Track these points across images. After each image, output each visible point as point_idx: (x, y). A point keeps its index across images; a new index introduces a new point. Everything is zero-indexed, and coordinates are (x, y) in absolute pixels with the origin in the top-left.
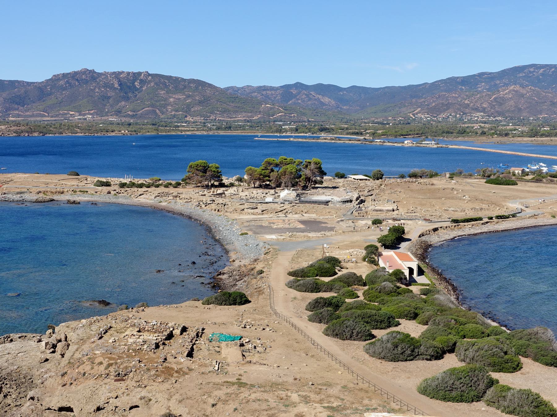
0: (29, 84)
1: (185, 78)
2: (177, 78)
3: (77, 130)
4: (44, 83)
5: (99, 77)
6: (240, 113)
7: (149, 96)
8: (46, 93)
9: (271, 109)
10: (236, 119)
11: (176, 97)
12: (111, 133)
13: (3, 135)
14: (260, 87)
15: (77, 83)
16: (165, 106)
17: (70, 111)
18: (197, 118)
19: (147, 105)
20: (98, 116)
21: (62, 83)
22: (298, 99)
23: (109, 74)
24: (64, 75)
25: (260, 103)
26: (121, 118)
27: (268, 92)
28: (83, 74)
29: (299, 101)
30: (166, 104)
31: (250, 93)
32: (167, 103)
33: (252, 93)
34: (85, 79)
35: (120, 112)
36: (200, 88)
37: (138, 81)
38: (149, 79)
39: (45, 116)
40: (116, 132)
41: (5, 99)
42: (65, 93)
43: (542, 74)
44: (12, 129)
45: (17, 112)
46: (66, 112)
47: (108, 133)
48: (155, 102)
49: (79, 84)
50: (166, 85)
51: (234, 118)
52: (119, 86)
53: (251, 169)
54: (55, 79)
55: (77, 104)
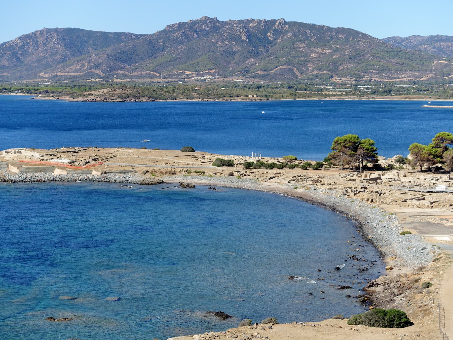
0: (137, 37)
1: (331, 26)
2: (321, 27)
3: (193, 94)
4: (155, 36)
5: (223, 27)
8: (157, 48)
9: (446, 66)
10: (398, 80)
11: (320, 51)
12: (236, 98)
13: (105, 100)
14: (432, 37)
16: (305, 63)
17: (186, 70)
18: (346, 79)
20: (220, 77)
21: (177, 35)
23: (236, 23)
24: (181, 26)
25: (431, 58)
26: (248, 79)
27: (442, 44)
28: (203, 24)
30: (306, 61)
32: (308, 59)
33: (421, 45)
34: (205, 30)
35: (247, 71)
36: (351, 39)
37: (271, 31)
38: (285, 29)
39: (156, 77)
40: (242, 97)
41: (109, 56)
42: (180, 48)
44: (116, 92)
45: (123, 72)
46: (181, 71)
47: (232, 98)
48: (292, 58)
49: (198, 37)
50: (307, 36)
51: (396, 78)
52: (247, 38)
53: (417, 146)
54: (169, 30)
55: (194, 62)
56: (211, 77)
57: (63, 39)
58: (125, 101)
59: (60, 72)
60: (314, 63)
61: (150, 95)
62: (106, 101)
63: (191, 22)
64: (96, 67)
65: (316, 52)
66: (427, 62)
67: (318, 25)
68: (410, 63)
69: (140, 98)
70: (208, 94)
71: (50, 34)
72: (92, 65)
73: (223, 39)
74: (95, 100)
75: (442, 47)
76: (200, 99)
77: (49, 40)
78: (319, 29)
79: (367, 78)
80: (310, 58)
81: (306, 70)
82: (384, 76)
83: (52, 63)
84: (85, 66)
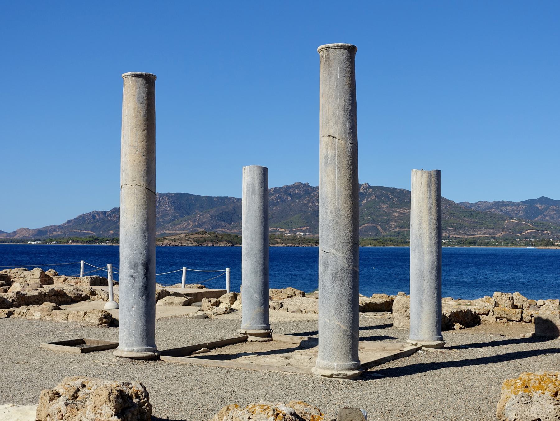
3: (277, 240)
5: (314, 191)
6: (480, 230)
7: (369, 211)
10: (474, 236)
11: (401, 211)
13: (180, 245)
14: (498, 202)
15: (289, 198)
16: (388, 221)
17: (280, 228)
19: (366, 220)
20: (310, 234)
22: (546, 216)
25: (503, 218)
27: (508, 208)
28: (296, 189)
29: (548, 218)
30: (389, 220)
31: (485, 209)
32: (390, 218)
33: (489, 208)
34: (298, 194)
38: (369, 192)
41: (212, 216)
44: (192, 237)
45: (223, 230)
46: (275, 229)
48: (376, 217)
49: (292, 199)
50: (389, 198)
51: (472, 235)
55: (287, 221)
56: (302, 234)
57: (173, 202)
58: (202, 245)
59: (168, 230)
60: (396, 221)
61: (230, 239)
62: (181, 246)
63: (286, 187)
64: (200, 226)
65: (397, 212)
66: (499, 221)
67: (399, 189)
68: (484, 222)
69: (218, 243)
70: (292, 240)
71: (162, 198)
72: (196, 224)
73: (314, 200)
74: (169, 244)
75: (508, 211)
76: (283, 245)
77: (161, 203)
78: (399, 193)
79: (445, 234)
80: (392, 218)
81: (389, 227)
82: (461, 233)
83: (162, 223)
84: (191, 224)
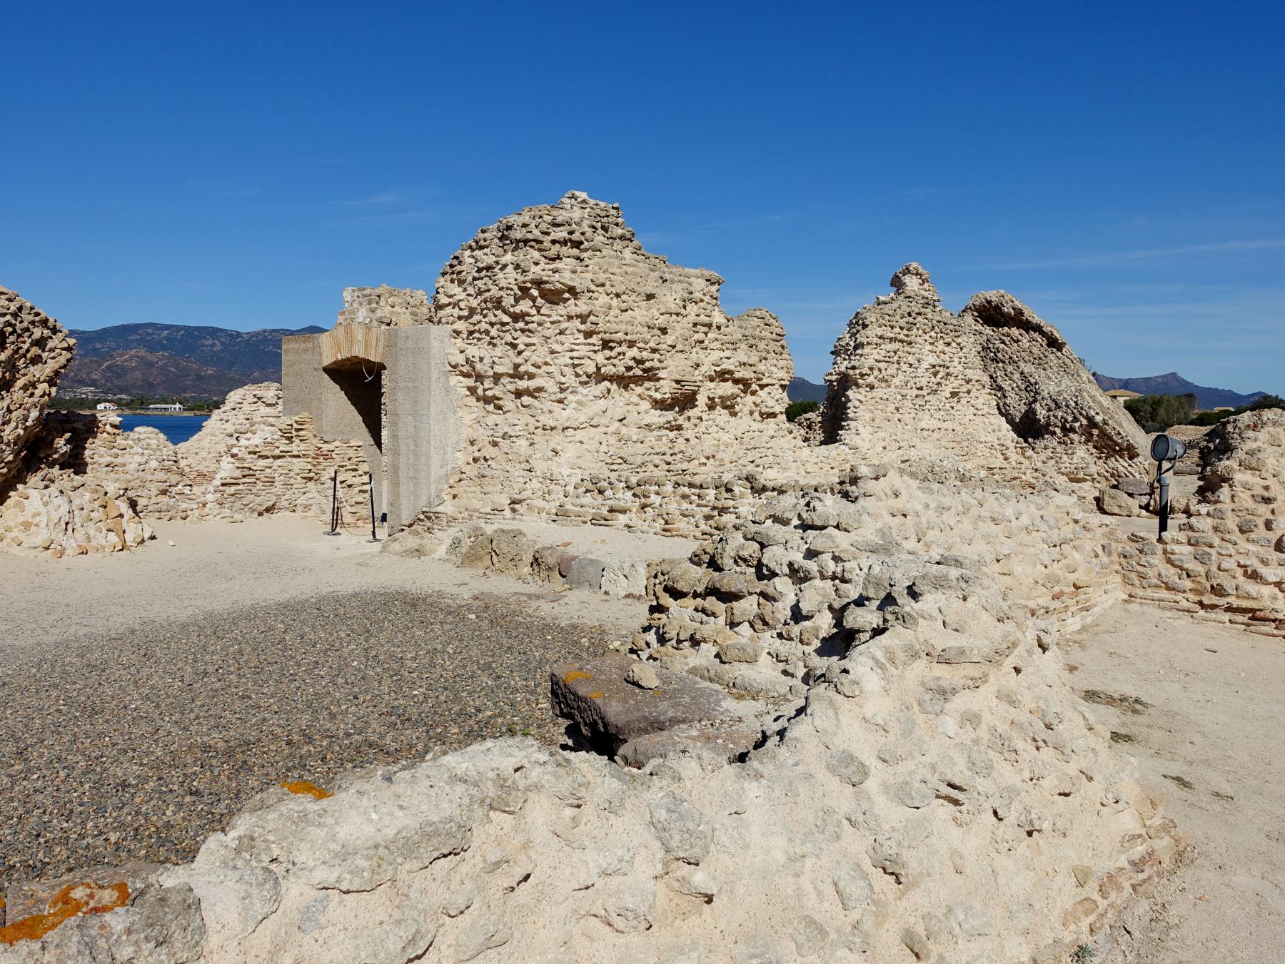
43: (166, 338)
